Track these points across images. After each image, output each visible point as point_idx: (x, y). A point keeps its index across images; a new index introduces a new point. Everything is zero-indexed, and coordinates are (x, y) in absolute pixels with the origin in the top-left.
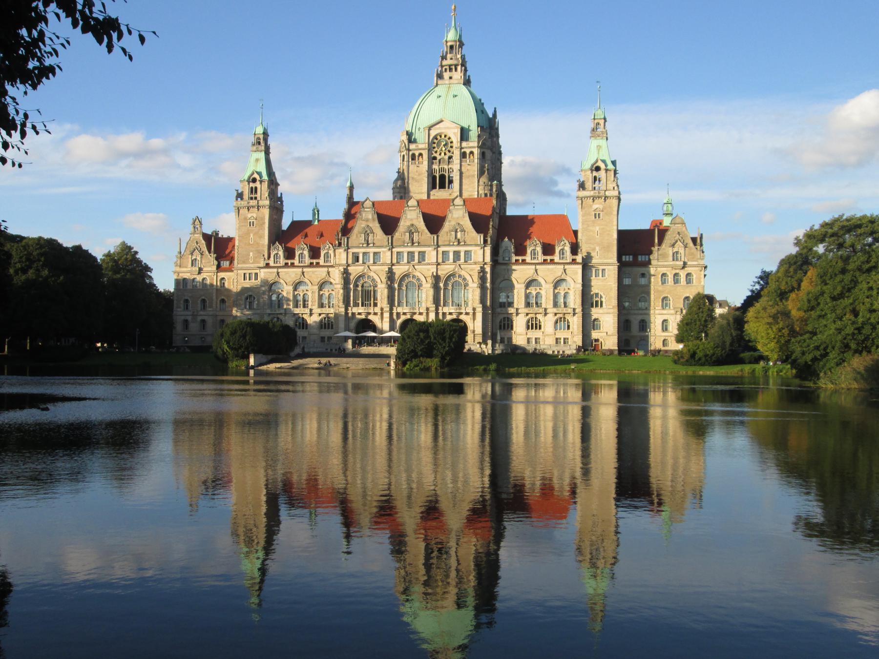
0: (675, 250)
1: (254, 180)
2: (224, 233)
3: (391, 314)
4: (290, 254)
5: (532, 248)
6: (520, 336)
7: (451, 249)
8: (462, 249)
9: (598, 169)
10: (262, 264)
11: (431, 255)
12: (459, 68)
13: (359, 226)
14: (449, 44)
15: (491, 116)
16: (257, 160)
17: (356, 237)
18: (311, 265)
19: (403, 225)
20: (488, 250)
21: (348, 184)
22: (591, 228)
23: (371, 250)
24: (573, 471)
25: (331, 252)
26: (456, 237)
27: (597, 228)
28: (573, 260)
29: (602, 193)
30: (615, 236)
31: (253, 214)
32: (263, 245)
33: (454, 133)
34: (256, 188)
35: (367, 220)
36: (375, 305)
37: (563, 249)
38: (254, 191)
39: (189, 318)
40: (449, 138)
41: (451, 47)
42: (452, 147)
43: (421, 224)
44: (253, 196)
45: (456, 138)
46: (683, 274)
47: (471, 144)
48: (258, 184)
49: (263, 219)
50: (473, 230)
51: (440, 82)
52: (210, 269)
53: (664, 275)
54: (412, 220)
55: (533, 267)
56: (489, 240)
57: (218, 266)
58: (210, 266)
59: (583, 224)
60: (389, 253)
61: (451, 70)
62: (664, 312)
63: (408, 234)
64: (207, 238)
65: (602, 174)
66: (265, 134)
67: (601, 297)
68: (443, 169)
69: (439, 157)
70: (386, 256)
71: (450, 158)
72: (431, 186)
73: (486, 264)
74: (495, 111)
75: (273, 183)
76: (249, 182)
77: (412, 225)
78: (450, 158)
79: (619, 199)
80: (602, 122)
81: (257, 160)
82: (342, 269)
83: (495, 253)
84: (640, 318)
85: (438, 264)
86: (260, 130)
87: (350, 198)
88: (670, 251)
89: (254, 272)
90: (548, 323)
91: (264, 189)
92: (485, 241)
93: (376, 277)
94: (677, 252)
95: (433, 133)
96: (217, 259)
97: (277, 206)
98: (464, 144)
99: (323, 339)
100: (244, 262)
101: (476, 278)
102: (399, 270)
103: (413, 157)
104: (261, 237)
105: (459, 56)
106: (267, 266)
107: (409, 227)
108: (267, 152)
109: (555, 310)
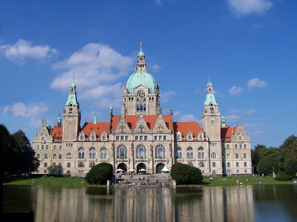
0: (240, 136)
1: (71, 105)
3: (134, 161)
5: (189, 135)
7: (158, 135)
8: (163, 135)
9: (212, 105)
10: (75, 140)
11: (150, 137)
12: (144, 66)
16: (72, 97)
17: (118, 130)
18: (97, 141)
19: (138, 125)
20: (173, 135)
21: (111, 108)
22: (211, 127)
23: (125, 135)
27: (213, 127)
28: (205, 139)
29: (214, 114)
30: (220, 130)
31: (71, 119)
32: (75, 132)
33: (146, 90)
34: (72, 109)
35: (123, 123)
36: (126, 157)
37: (201, 136)
41: (141, 58)
43: (145, 125)
44: (71, 112)
45: (146, 93)
47: (153, 95)
48: (73, 107)
50: (167, 128)
52: (49, 142)
53: (236, 145)
55: (190, 142)
56: (173, 131)
57: (53, 140)
58: (50, 140)
59: (207, 126)
61: (141, 67)
62: (237, 159)
67: (215, 154)
69: (140, 99)
70: (131, 138)
73: (172, 141)
76: (69, 106)
78: (145, 100)
81: (72, 97)
82: (112, 142)
85: (153, 141)
87: (112, 113)
88: (238, 136)
89: (71, 143)
91: (75, 109)
92: (172, 132)
93: (126, 146)
94: (240, 137)
95: (137, 90)
98: (150, 95)
100: (67, 139)
101: (168, 147)
104: (75, 128)
105: (144, 62)
106: (78, 141)
109: (199, 159)
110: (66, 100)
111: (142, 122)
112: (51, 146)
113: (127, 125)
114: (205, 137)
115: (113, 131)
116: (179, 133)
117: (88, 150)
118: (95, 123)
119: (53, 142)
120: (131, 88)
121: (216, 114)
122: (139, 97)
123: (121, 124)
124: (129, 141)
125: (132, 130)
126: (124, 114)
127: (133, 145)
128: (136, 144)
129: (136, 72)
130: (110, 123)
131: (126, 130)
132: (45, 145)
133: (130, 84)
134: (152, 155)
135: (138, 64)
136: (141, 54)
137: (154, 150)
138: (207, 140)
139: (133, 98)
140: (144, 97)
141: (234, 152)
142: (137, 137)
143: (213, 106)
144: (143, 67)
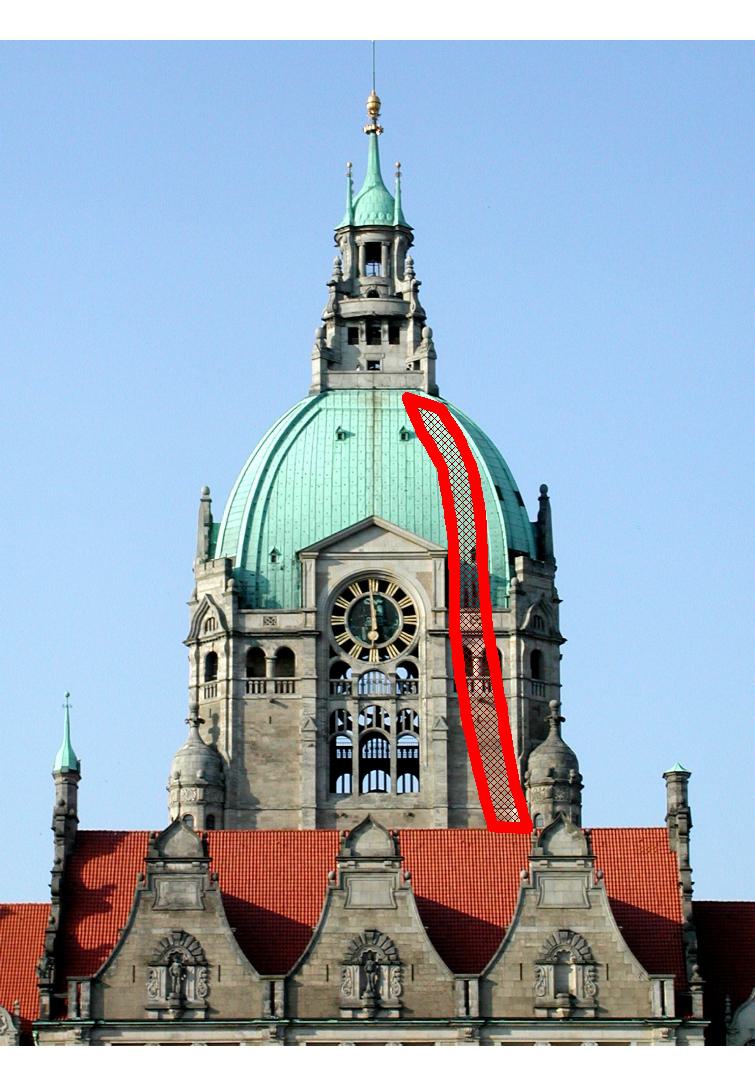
12: (408, 334)
14: (363, 239)
15: (532, 513)
21: (61, 762)
26: (560, 988)
33: (421, 576)
35: (179, 909)
40: (400, 595)
41: (373, 253)
42: (410, 629)
43: (410, 932)
50: (629, 959)
51: (334, 380)
54: (370, 910)
56: (698, 999)
61: (373, 338)
63: (354, 971)
74: (544, 500)
77: (375, 933)
87: (67, 815)
92: (683, 1004)
95: (337, 574)
103: (253, 662)
107: (358, 943)
111: (374, 902)
113: (225, 931)
115: (86, 994)
120: (274, 555)
122: (348, 646)
123: (161, 926)
125: (279, 987)
126: (197, 823)
129: (325, 390)
130: (56, 912)
131: (213, 983)
133: (258, 515)
135: (350, 308)
139: (285, 658)
140: (400, 645)
144: (394, 338)
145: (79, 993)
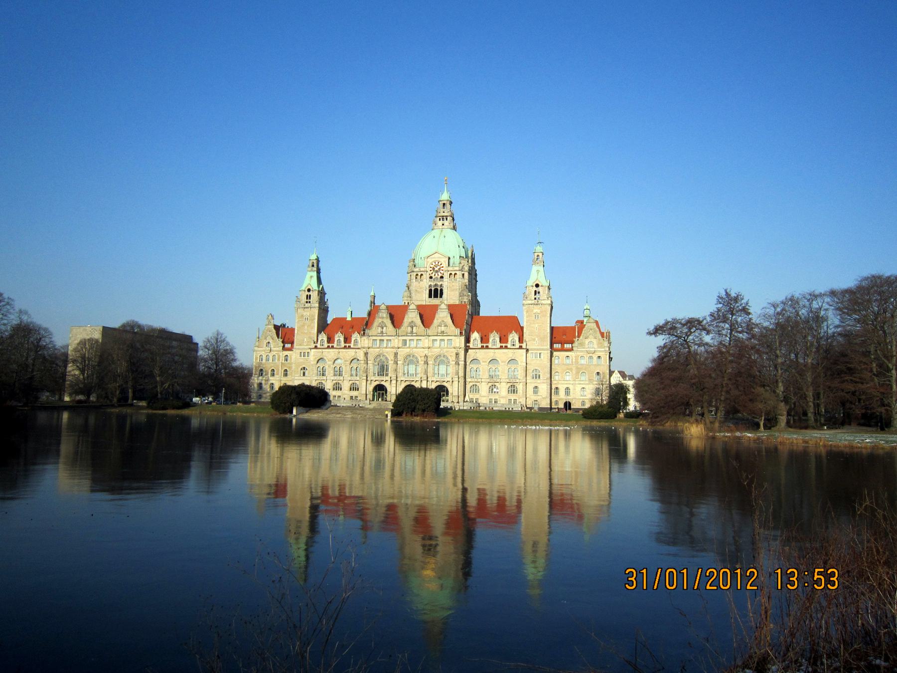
1: (309, 290)
2: (289, 325)
4: (330, 340)
6: (484, 398)
7: (438, 338)
8: (446, 338)
9: (537, 286)
13: (377, 321)
17: (375, 330)
19: (407, 320)
20: (463, 339)
21: (372, 294)
23: (385, 338)
24: (519, 492)
25: (359, 339)
30: (549, 330)
31: (307, 313)
36: (387, 375)
38: (308, 297)
39: (263, 382)
41: (444, 204)
43: (418, 321)
45: (445, 264)
46: (595, 357)
48: (311, 293)
49: (313, 316)
57: (284, 346)
60: (396, 341)
64: (277, 328)
65: (540, 289)
66: (318, 260)
68: (436, 285)
70: (396, 342)
71: (442, 277)
72: (427, 296)
75: (322, 293)
78: (442, 277)
79: (552, 308)
80: (540, 255)
83: (468, 340)
84: (566, 386)
86: (314, 257)
87: (373, 303)
90: (503, 389)
91: (315, 296)
95: (430, 260)
96: (283, 342)
97: (324, 310)
98: (450, 269)
99: (352, 397)
101: (454, 358)
102: (403, 352)
106: (316, 347)
108: (318, 271)
110: (302, 282)
112: (279, 356)
114: (521, 340)
116: (475, 336)
117: (331, 363)
118: (349, 319)
119: (284, 349)
121: (543, 302)
123: (380, 320)
124: (393, 348)
127: (396, 354)
128: (403, 352)
132: (271, 355)
134: (426, 372)
136: (445, 197)
137: (431, 362)
138: (524, 346)
141: (577, 368)
142: (405, 342)
143: (540, 289)
145: (367, 331)
